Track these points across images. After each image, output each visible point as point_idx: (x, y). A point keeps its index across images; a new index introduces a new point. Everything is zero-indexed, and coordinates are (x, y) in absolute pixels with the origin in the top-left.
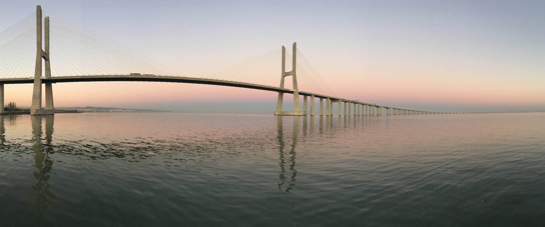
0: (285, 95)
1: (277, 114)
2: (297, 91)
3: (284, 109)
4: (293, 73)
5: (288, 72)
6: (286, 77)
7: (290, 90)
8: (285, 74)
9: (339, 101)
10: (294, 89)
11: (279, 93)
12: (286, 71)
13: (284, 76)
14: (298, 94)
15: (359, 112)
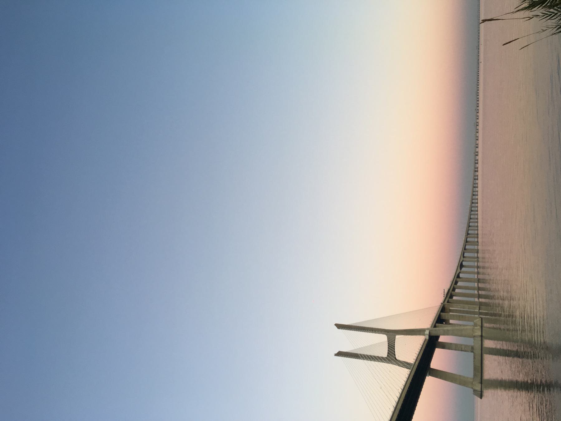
0: (434, 364)
1: (478, 388)
2: (428, 329)
3: (469, 373)
4: (391, 334)
5: (388, 346)
6: (397, 358)
7: (427, 337)
8: (391, 358)
9: (446, 306)
10: (424, 335)
11: (430, 375)
12: (384, 353)
13: (396, 359)
14: (435, 329)
15: (474, 289)
